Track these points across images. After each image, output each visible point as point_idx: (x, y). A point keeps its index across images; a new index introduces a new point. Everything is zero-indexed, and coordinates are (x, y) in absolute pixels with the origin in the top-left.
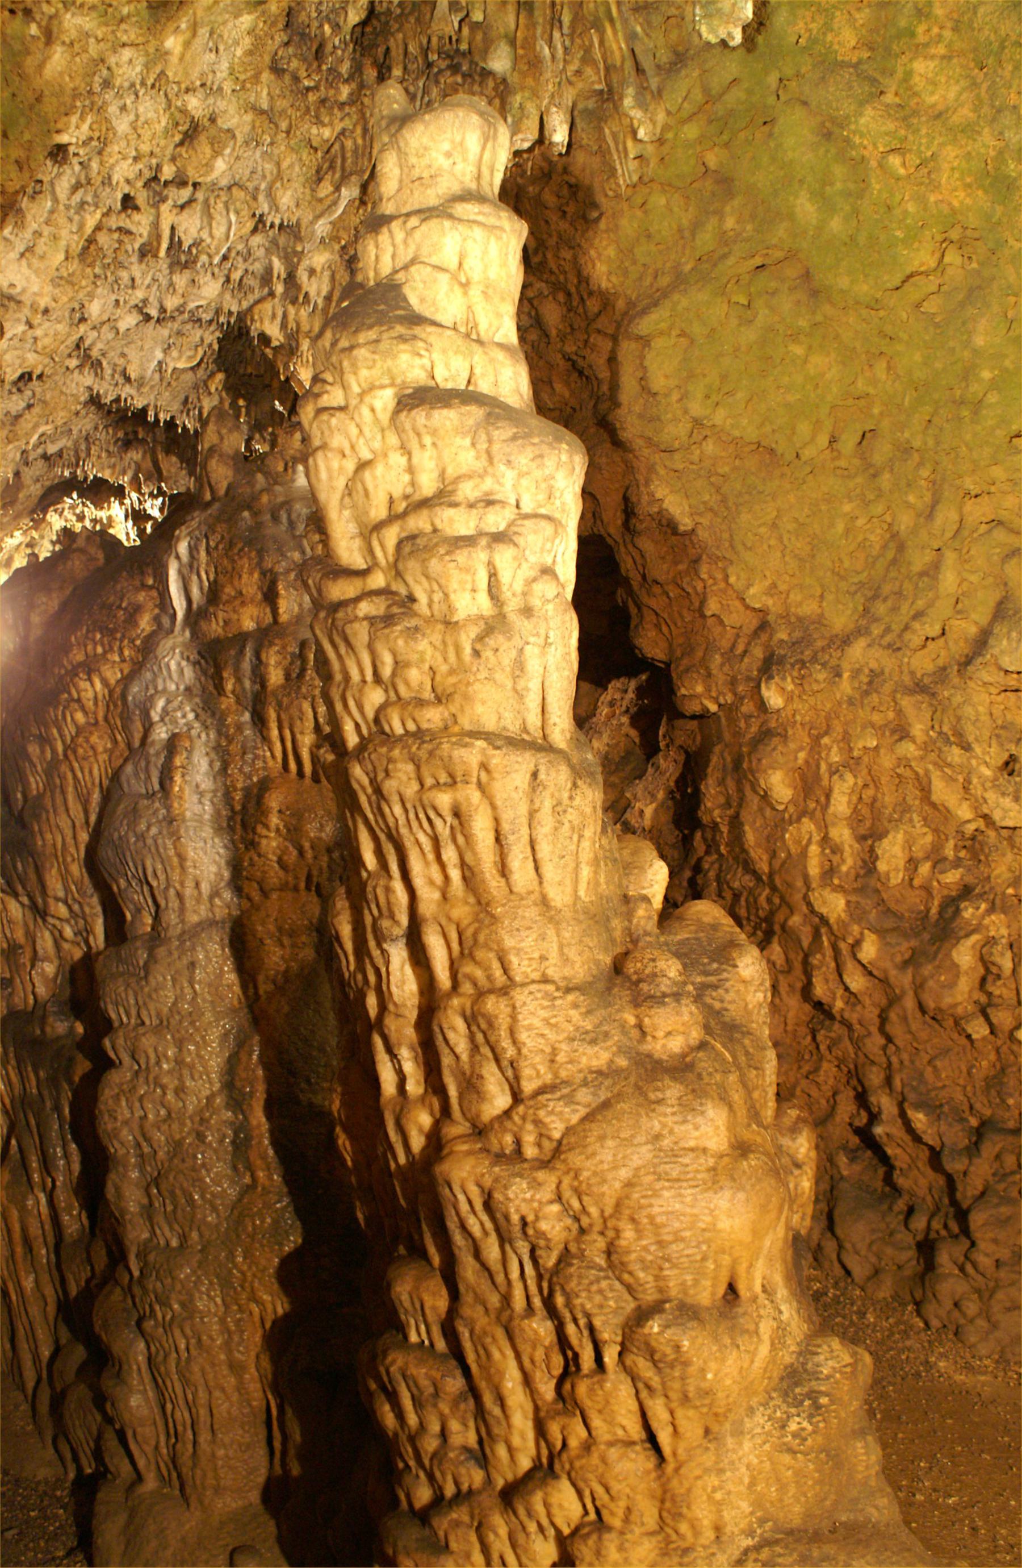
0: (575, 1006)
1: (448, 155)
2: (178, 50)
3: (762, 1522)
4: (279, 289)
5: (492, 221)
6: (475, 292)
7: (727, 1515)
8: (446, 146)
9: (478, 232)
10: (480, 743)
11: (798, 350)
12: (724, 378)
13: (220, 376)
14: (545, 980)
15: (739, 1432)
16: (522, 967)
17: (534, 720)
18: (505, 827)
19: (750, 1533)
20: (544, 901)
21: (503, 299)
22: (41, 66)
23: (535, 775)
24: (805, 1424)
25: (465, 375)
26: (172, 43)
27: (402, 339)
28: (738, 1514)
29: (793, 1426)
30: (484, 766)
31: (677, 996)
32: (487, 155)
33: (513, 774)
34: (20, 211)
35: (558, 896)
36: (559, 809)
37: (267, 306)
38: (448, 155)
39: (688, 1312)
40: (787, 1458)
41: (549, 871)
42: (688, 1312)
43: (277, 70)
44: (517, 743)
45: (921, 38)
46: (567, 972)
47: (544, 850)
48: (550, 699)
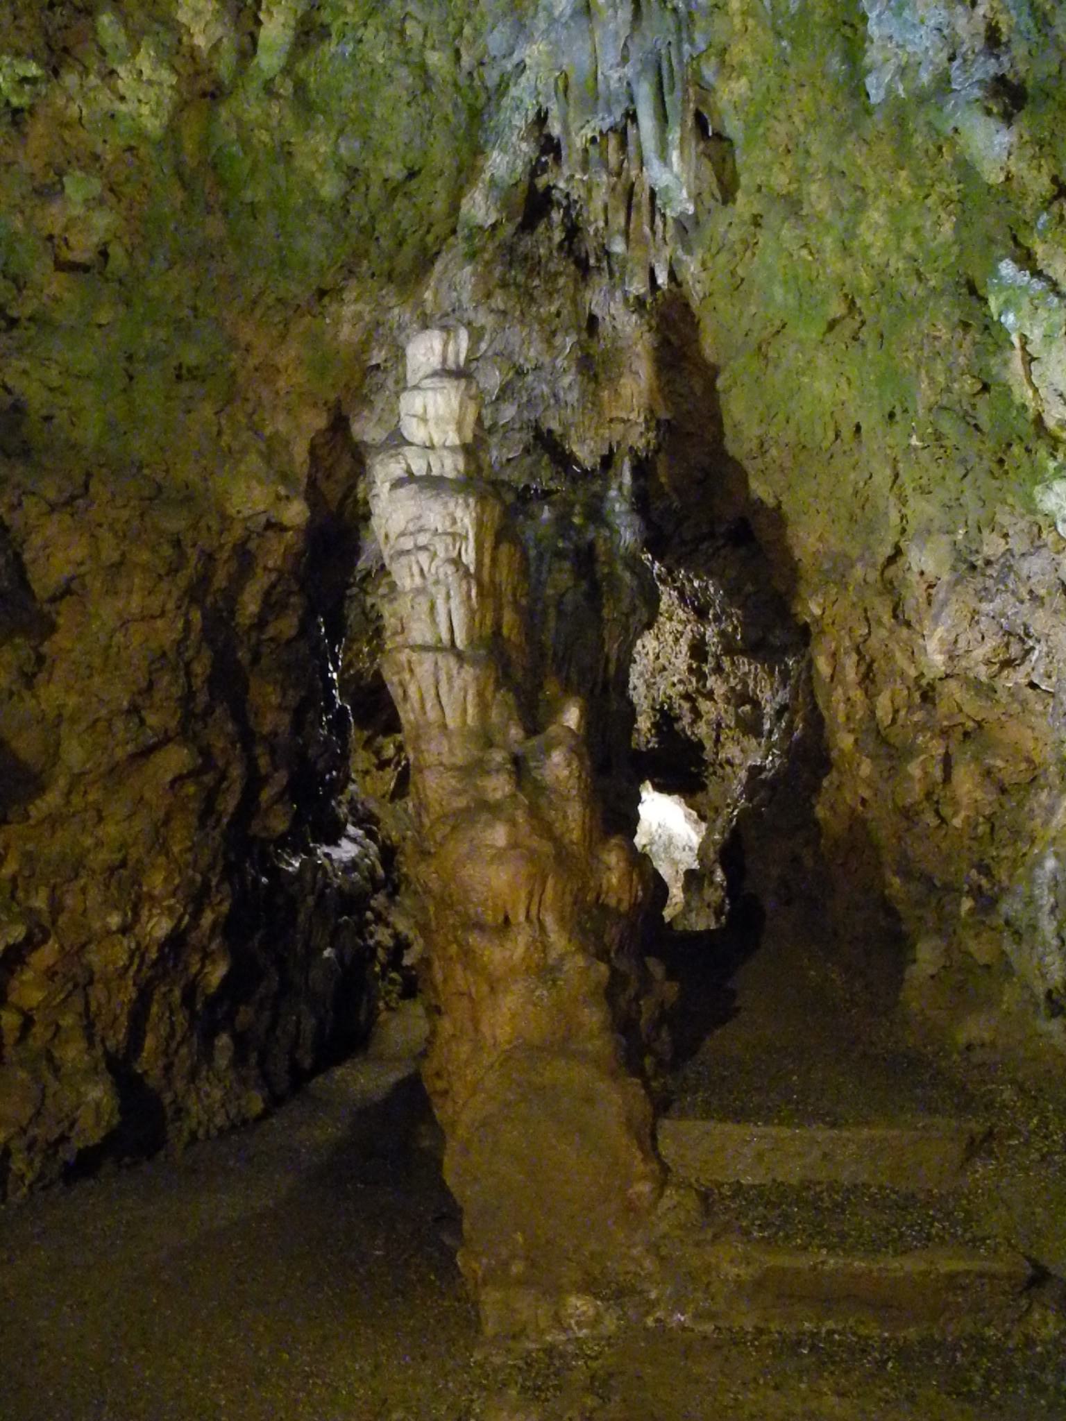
0: (454, 777)
1: (425, 355)
2: (431, 298)
3: (517, 1038)
4: (552, 401)
5: (440, 385)
6: (431, 423)
7: (498, 1032)
8: (423, 351)
9: (430, 394)
10: (407, 650)
11: (806, 380)
12: (768, 407)
13: (546, 457)
14: (441, 764)
15: (506, 990)
16: (430, 758)
17: (445, 636)
18: (424, 689)
19: (510, 1042)
20: (444, 726)
21: (448, 424)
22: (335, 337)
23: (436, 663)
24: (545, 993)
25: (425, 467)
26: (428, 295)
27: (392, 456)
28: (504, 1033)
29: (537, 993)
30: (409, 662)
31: (498, 771)
32: (451, 348)
33: (425, 665)
34: (371, 402)
35: (452, 723)
36: (450, 679)
37: (549, 413)
38: (425, 355)
39: (480, 926)
40: (530, 1007)
41: (447, 710)
42: (480, 926)
43: (504, 285)
44: (425, 648)
45: (811, 171)
46: (453, 760)
47: (444, 700)
48: (455, 624)
